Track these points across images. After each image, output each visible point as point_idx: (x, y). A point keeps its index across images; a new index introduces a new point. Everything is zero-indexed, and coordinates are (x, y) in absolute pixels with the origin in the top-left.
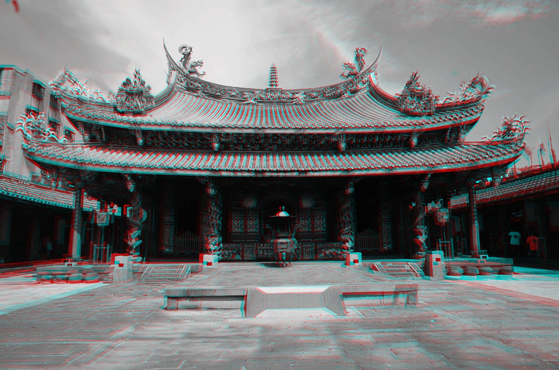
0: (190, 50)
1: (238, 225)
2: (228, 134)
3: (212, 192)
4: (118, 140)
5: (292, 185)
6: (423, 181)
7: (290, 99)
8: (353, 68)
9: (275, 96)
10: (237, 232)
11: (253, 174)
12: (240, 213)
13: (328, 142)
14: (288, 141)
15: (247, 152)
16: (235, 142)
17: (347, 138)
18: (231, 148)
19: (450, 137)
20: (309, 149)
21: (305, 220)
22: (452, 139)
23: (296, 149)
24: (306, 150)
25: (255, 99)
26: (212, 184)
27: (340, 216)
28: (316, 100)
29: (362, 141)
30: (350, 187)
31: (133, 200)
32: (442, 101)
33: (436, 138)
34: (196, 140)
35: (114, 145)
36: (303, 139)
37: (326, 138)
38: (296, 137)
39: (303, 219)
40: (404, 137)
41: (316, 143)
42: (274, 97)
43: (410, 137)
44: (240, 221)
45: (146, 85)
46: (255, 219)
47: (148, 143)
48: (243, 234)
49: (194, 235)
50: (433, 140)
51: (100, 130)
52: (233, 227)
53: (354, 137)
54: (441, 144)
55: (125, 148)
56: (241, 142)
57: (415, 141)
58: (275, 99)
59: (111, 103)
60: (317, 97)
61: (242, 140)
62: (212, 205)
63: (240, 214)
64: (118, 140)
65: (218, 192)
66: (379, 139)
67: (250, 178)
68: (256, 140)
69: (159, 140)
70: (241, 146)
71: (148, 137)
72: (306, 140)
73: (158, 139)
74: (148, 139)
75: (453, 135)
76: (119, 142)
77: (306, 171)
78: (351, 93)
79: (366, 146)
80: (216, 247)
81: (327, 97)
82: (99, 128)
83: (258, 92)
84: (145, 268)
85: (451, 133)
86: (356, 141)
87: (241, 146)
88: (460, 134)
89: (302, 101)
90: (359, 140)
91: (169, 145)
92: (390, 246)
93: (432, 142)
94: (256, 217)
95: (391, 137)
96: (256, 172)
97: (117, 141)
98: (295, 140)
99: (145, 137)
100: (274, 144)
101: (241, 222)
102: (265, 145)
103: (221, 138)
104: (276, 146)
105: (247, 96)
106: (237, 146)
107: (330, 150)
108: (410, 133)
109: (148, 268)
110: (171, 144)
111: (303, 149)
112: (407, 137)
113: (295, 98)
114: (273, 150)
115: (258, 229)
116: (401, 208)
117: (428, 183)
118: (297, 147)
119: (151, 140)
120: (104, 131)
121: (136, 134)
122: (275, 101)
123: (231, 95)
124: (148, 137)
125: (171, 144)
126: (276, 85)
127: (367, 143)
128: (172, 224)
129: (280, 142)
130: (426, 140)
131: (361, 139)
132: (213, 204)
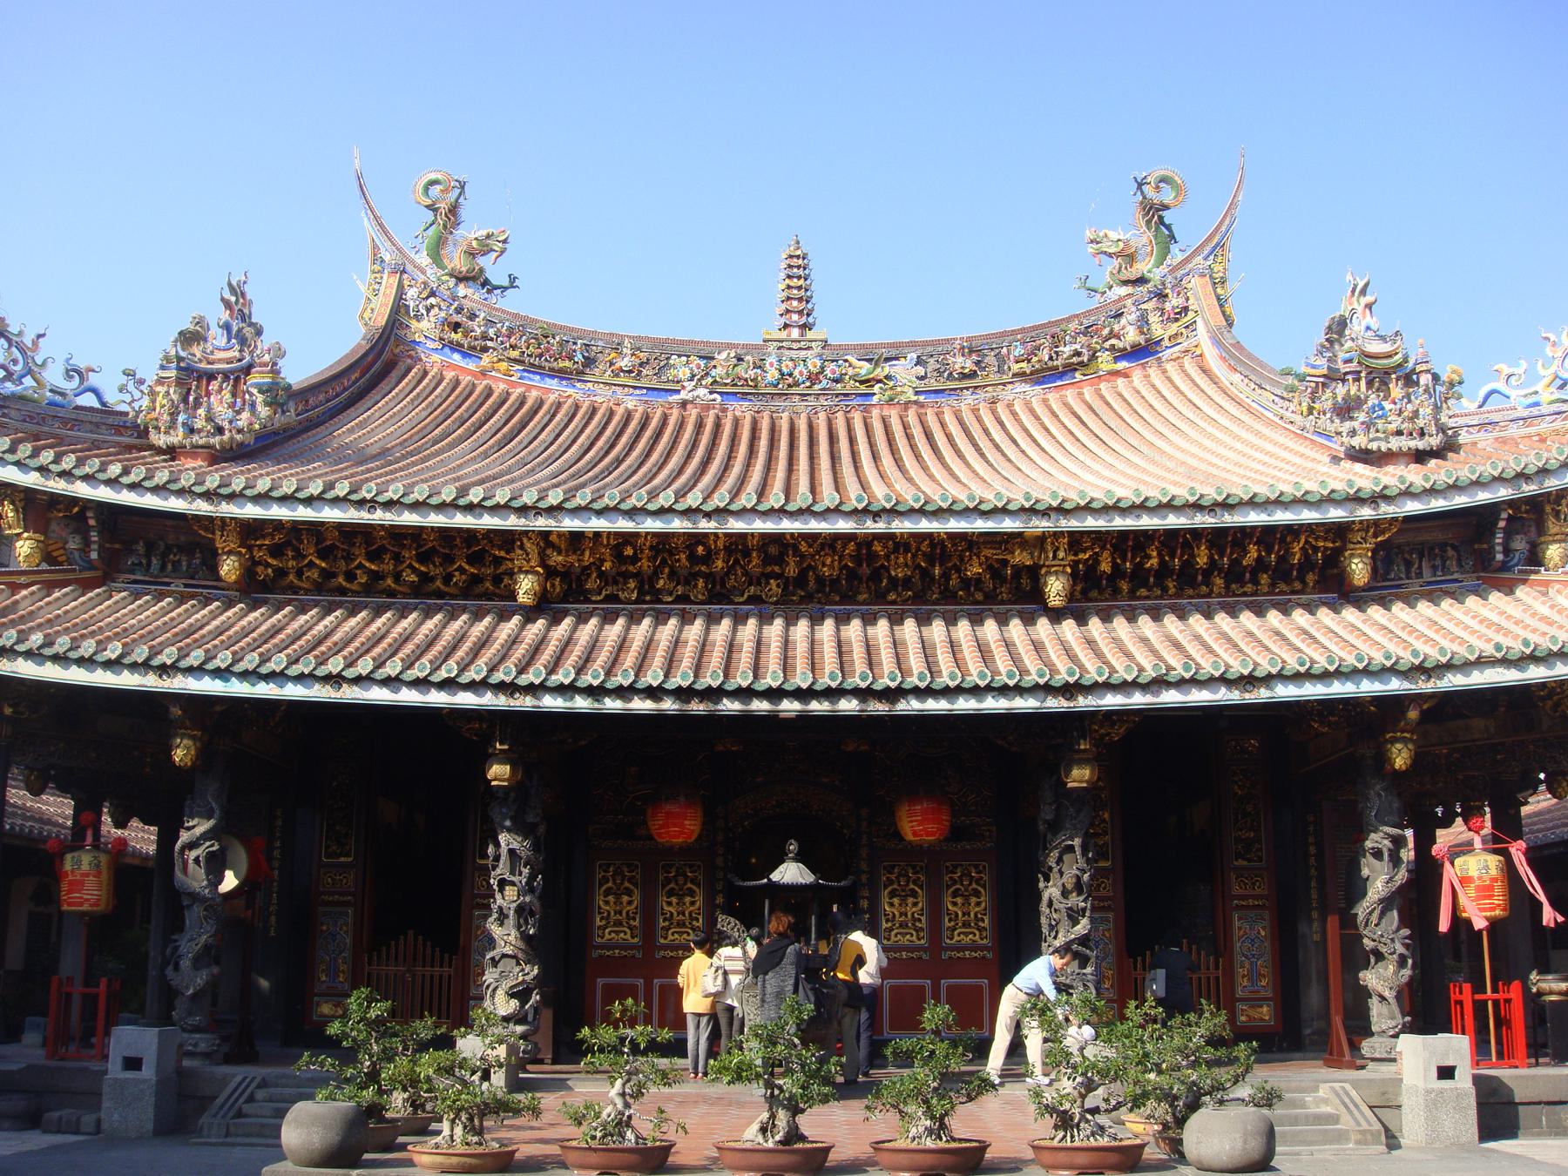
0: (457, 191)
1: (620, 914)
2: (576, 538)
4: (148, 556)
5: (851, 748)
6: (1388, 736)
7: (861, 382)
8: (1131, 258)
9: (796, 373)
10: (610, 946)
11: (669, 705)
12: (629, 866)
13: (996, 569)
14: (828, 567)
15: (654, 609)
16: (607, 565)
17: (1076, 554)
18: (589, 591)
19: (1507, 551)
20: (919, 598)
21: (903, 902)
22: (1515, 561)
23: (861, 598)
24: (905, 602)
25: (715, 382)
27: (1041, 885)
28: (967, 388)
29: (1141, 564)
30: (1081, 763)
31: (188, 802)
32: (1471, 400)
33: (1451, 552)
34: (449, 559)
35: (133, 577)
36: (887, 557)
37: (988, 552)
38: (859, 545)
39: (892, 894)
40: (1316, 549)
41: (946, 576)
42: (790, 375)
43: (1339, 552)
44: (625, 898)
45: (266, 341)
46: (690, 889)
47: (260, 569)
48: (639, 955)
49: (433, 948)
50: (1438, 562)
51: (82, 517)
52: (598, 923)
53: (1103, 548)
55: (172, 588)
56: (631, 568)
57: (1358, 569)
58: (797, 384)
59: (124, 408)
60: (973, 375)
61: (635, 559)
62: (504, 827)
63: (626, 870)
64: (148, 556)
66: (1211, 558)
68: (693, 558)
69: (304, 557)
70: (632, 585)
71: (260, 547)
72: (901, 560)
73: (299, 556)
74: (258, 554)
75: (1520, 544)
76: (149, 564)
77: (891, 695)
78: (1116, 359)
79: (1155, 585)
80: (514, 1003)
81: (1014, 375)
82: (77, 510)
83: (724, 355)
84: (224, 1081)
85: (1509, 534)
86: (1115, 566)
87: (632, 585)
88: (1543, 539)
89: (911, 391)
90: (1124, 561)
91: (341, 580)
92: (1265, 1012)
93: (1434, 568)
95: (1259, 551)
97: (144, 561)
98: (857, 559)
99: (250, 548)
100: (768, 576)
101: (632, 903)
102: (731, 583)
103: (549, 552)
104: (778, 586)
105: (684, 373)
106: (616, 582)
107: (1002, 602)
108: (1340, 531)
109: (238, 1079)
110: (350, 576)
111: (892, 596)
112: (1326, 548)
113: (880, 381)
114: (765, 602)
116: (1312, 850)
117: (1411, 746)
118: (863, 587)
119: (273, 556)
120: (97, 521)
121: (213, 533)
122: (794, 390)
123: (617, 365)
124: (260, 549)
125: (350, 576)
126: (805, 327)
127: (1163, 571)
128: (348, 904)
129: (792, 570)
130: (1408, 564)
131: (1133, 557)
132: (508, 823)
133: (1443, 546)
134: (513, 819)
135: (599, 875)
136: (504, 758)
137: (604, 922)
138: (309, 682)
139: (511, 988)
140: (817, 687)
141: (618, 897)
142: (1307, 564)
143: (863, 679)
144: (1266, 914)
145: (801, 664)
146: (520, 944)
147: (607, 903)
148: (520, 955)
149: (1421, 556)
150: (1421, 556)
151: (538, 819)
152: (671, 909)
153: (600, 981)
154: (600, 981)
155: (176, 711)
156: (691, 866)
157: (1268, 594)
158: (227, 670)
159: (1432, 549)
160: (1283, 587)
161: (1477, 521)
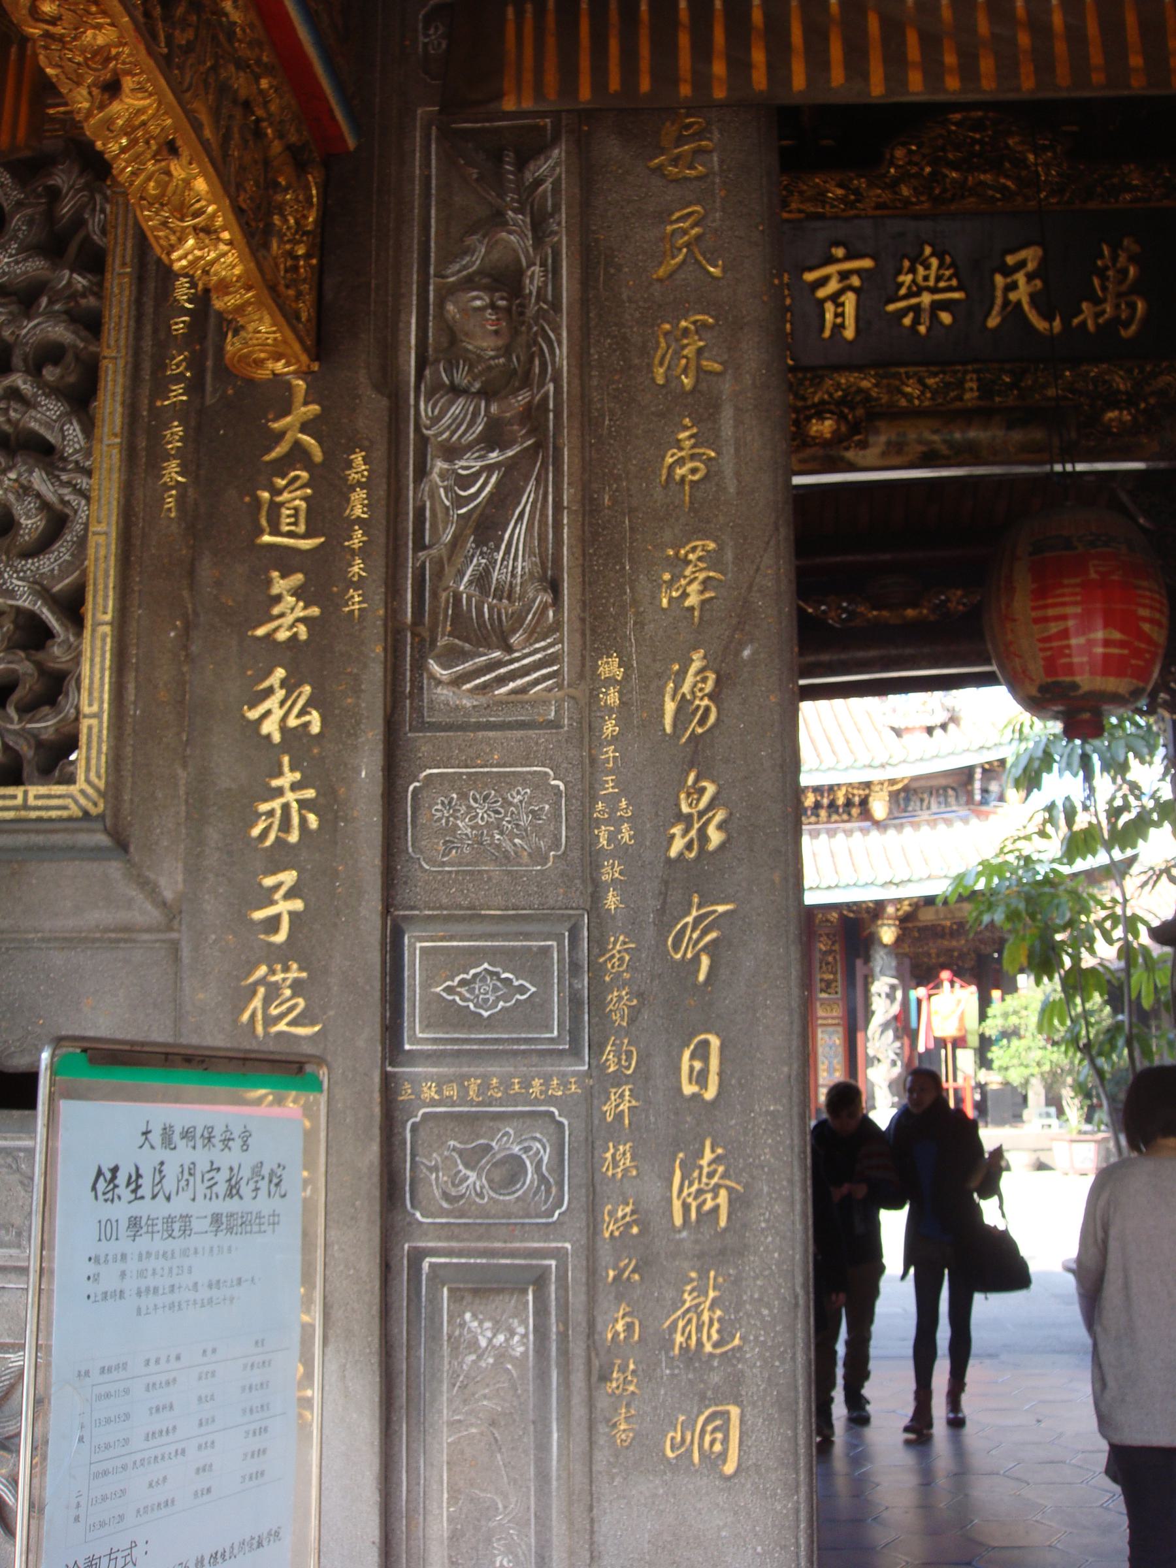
19: (985, 791)
33: (950, 792)
40: (854, 795)
50: (942, 799)
54: (963, 811)
57: (879, 807)
93: (939, 803)
108: (868, 785)
130: (922, 800)
133: (945, 789)
142: (849, 804)
144: (840, 1029)
149: (931, 794)
150: (931, 794)
157: (829, 822)
159: (937, 791)
160: (835, 817)
161: (967, 774)
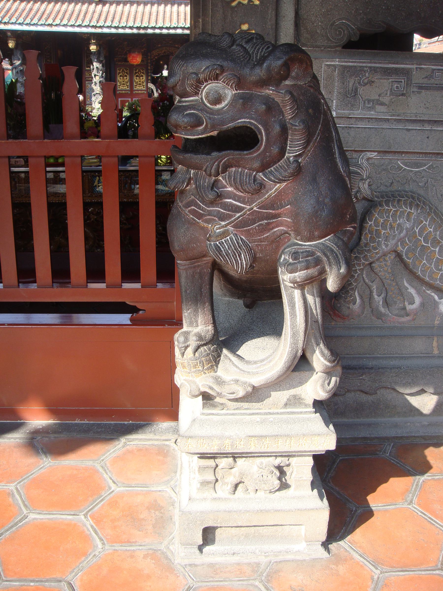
1: (124, 81)
3: (93, 48)
11: (135, 31)
12: (126, 69)
26: (94, 41)
31: (13, 57)
44: (125, 78)
48: (129, 92)
63: (125, 70)
65: (100, 48)
67: (133, 35)
94: (143, 73)
96: (139, 28)
101: (127, 79)
115: (145, 87)
132: (96, 60)
134: (97, 59)
135: (118, 72)
136: (95, 44)
137: (120, 84)
138: (44, 26)
139: (99, 101)
140: (172, 27)
141: (123, 77)
143: (183, 24)
145: (167, 19)
146: (101, 91)
147: (120, 79)
148: (101, 93)
151: (103, 59)
152: (137, 80)
153: (120, 99)
154: (120, 99)
155: (9, 34)
156: (142, 69)
158: (22, 23)
